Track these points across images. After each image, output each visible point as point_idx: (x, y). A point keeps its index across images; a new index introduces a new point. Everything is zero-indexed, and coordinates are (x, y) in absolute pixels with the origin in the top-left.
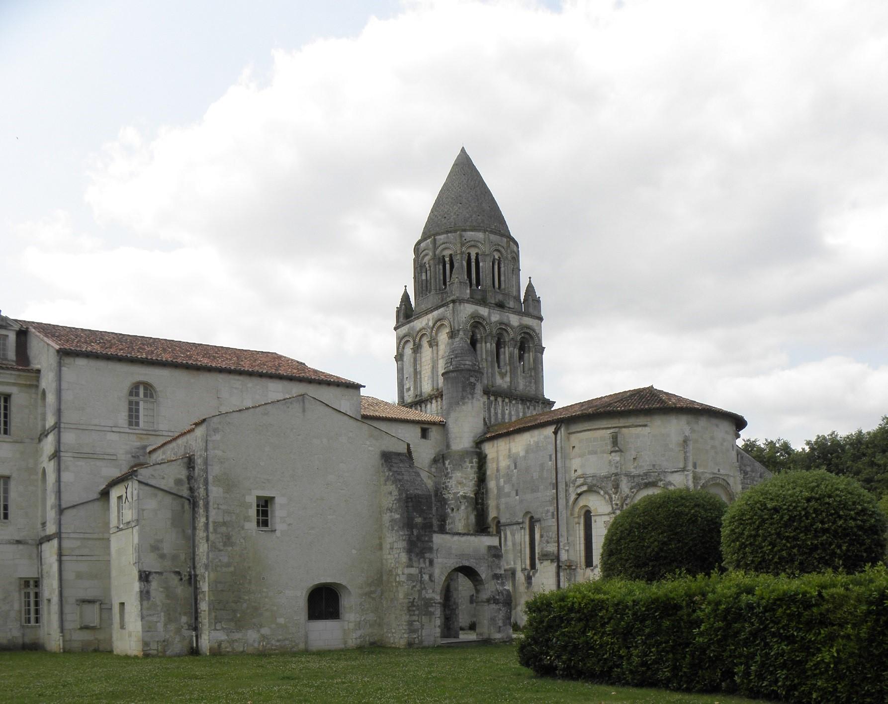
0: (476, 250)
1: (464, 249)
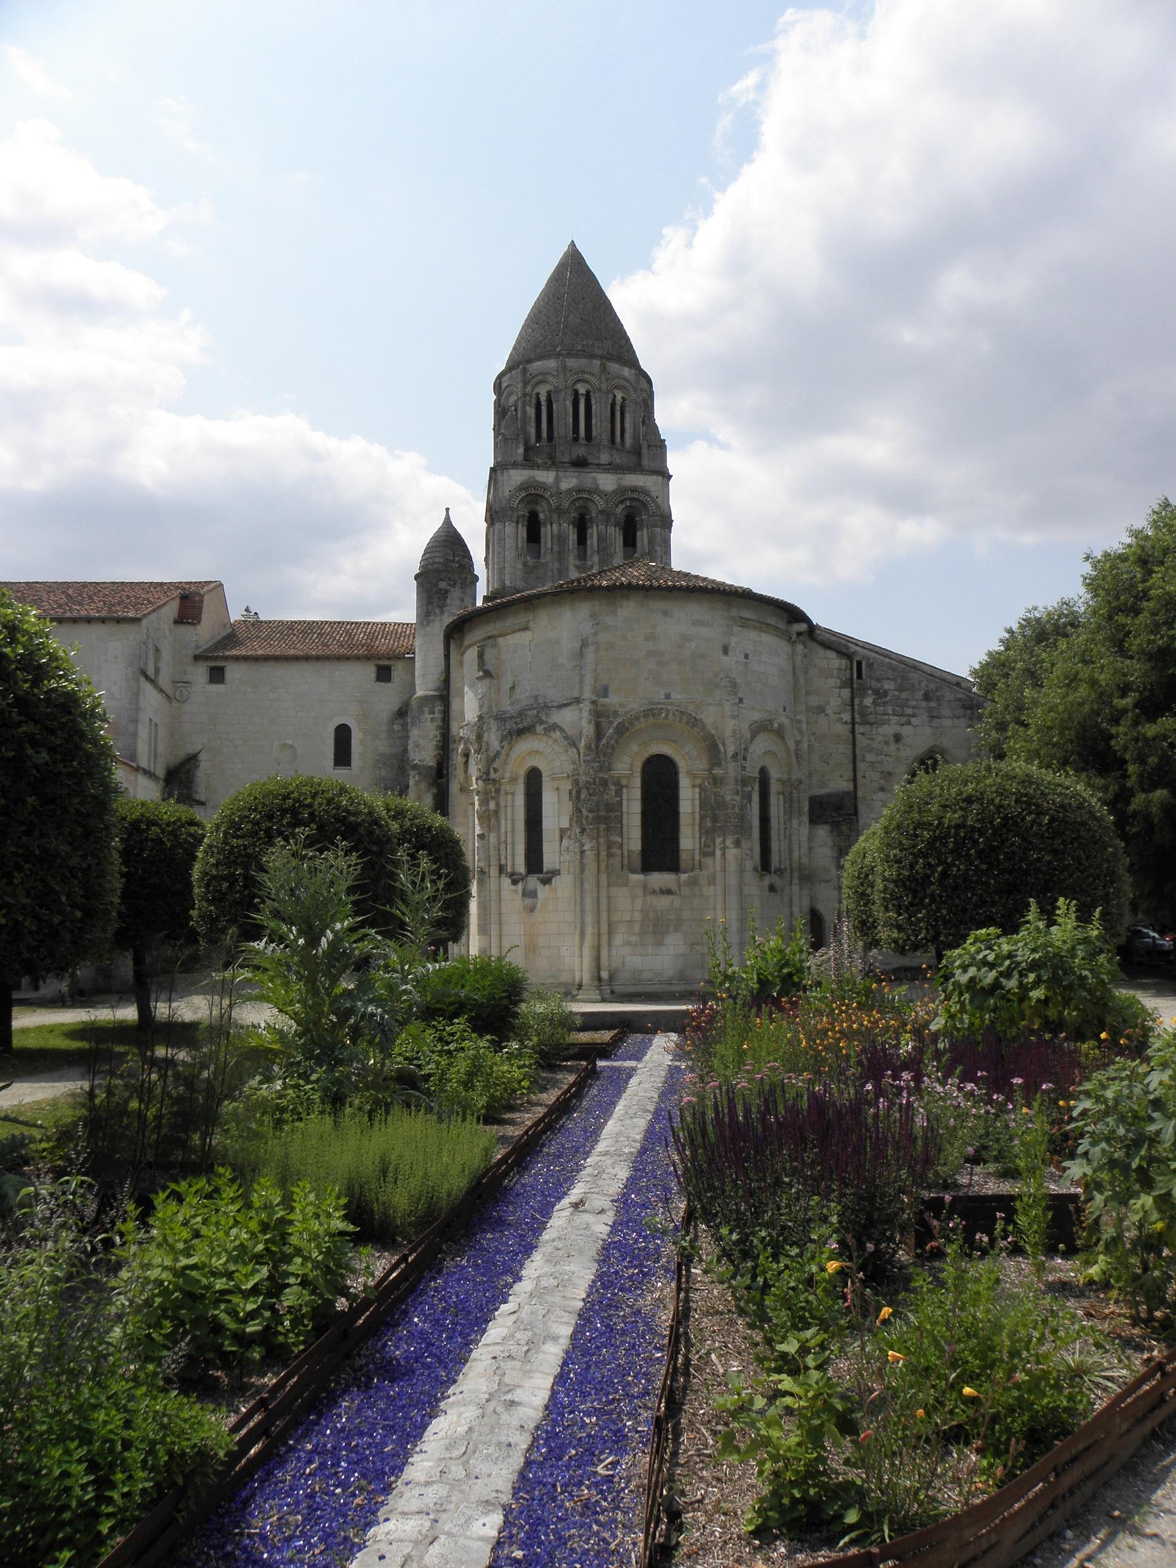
0: (588, 386)
1: (529, 389)
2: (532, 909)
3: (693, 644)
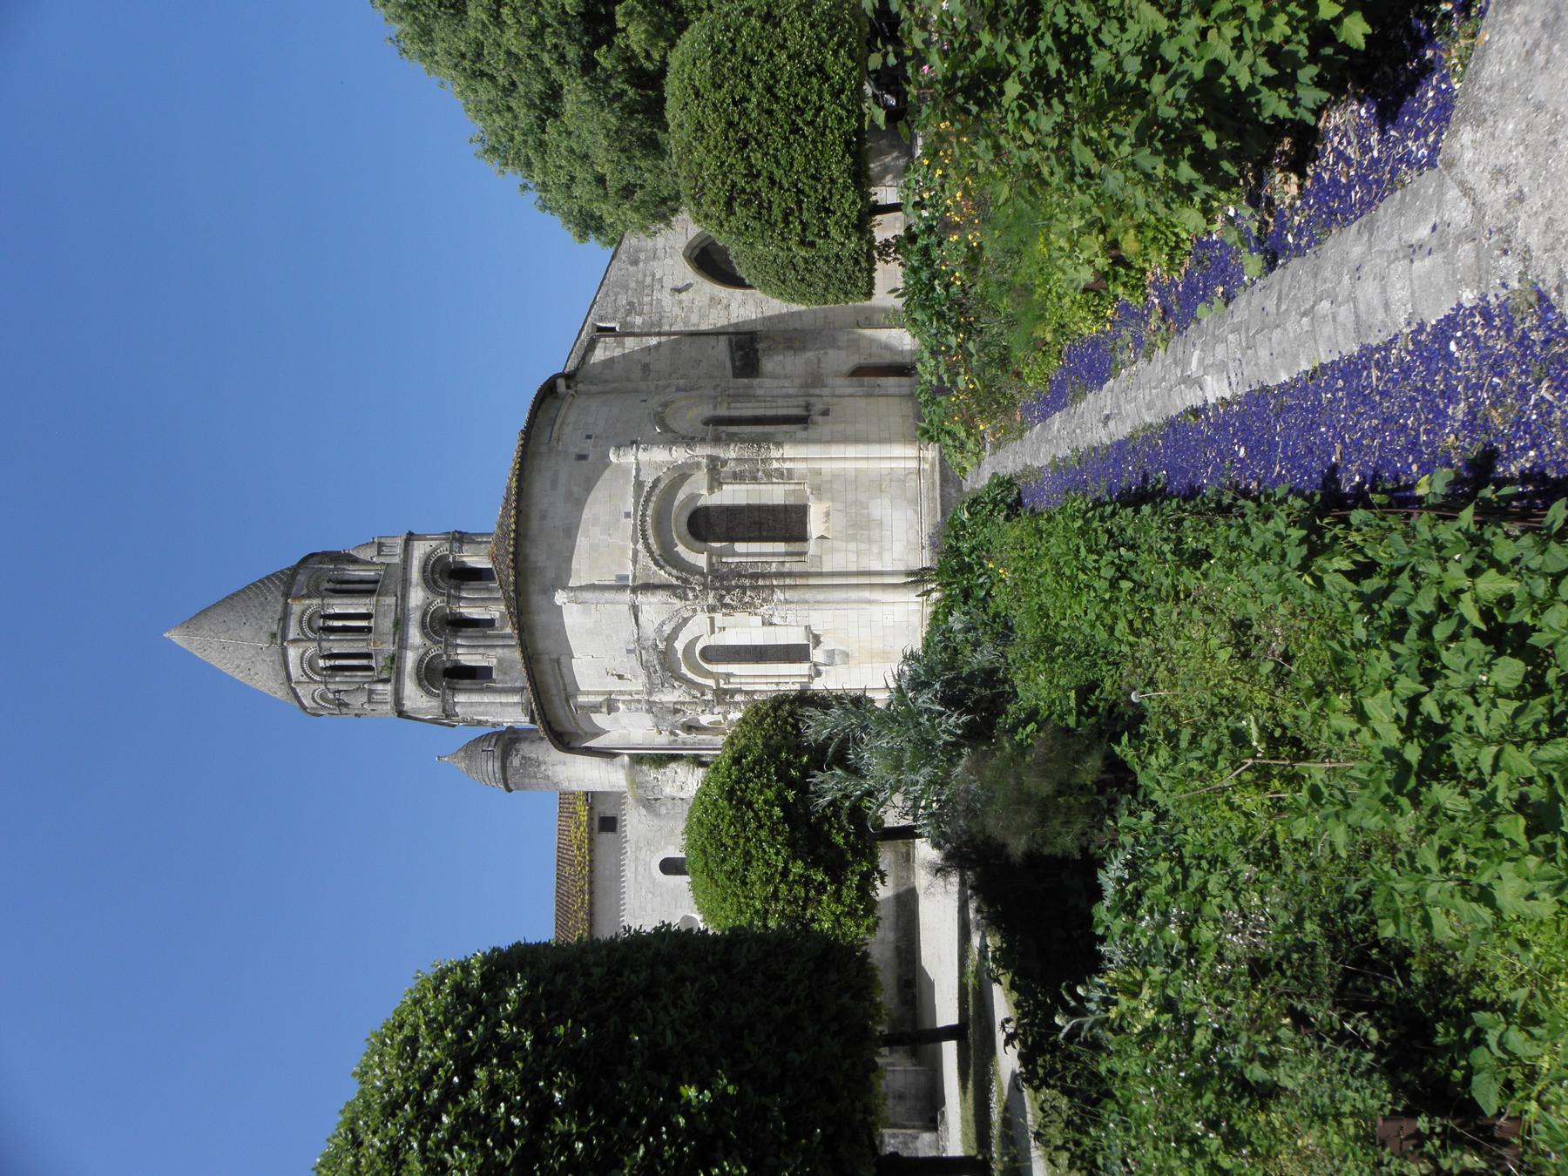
2: (846, 655)
3: (576, 490)
